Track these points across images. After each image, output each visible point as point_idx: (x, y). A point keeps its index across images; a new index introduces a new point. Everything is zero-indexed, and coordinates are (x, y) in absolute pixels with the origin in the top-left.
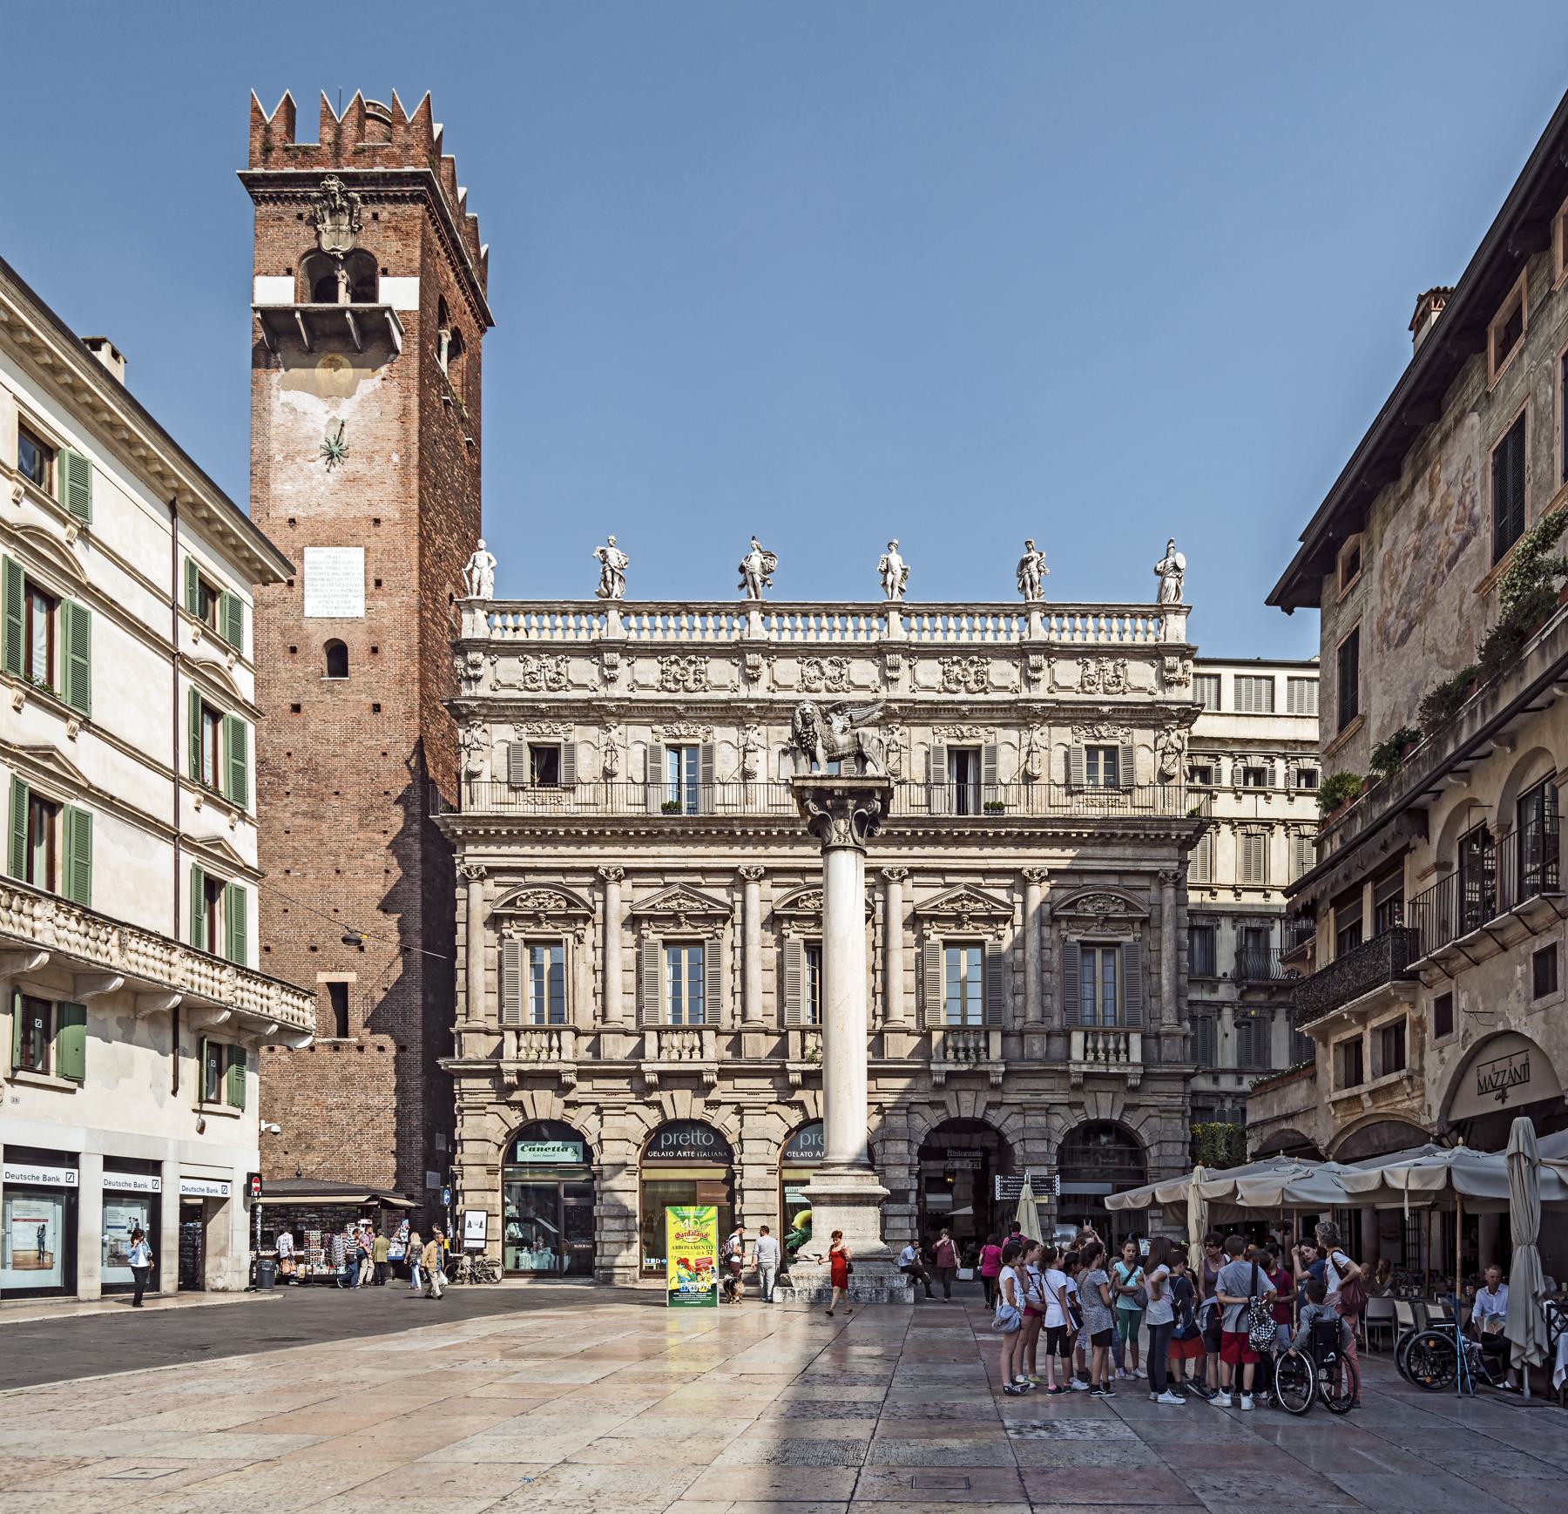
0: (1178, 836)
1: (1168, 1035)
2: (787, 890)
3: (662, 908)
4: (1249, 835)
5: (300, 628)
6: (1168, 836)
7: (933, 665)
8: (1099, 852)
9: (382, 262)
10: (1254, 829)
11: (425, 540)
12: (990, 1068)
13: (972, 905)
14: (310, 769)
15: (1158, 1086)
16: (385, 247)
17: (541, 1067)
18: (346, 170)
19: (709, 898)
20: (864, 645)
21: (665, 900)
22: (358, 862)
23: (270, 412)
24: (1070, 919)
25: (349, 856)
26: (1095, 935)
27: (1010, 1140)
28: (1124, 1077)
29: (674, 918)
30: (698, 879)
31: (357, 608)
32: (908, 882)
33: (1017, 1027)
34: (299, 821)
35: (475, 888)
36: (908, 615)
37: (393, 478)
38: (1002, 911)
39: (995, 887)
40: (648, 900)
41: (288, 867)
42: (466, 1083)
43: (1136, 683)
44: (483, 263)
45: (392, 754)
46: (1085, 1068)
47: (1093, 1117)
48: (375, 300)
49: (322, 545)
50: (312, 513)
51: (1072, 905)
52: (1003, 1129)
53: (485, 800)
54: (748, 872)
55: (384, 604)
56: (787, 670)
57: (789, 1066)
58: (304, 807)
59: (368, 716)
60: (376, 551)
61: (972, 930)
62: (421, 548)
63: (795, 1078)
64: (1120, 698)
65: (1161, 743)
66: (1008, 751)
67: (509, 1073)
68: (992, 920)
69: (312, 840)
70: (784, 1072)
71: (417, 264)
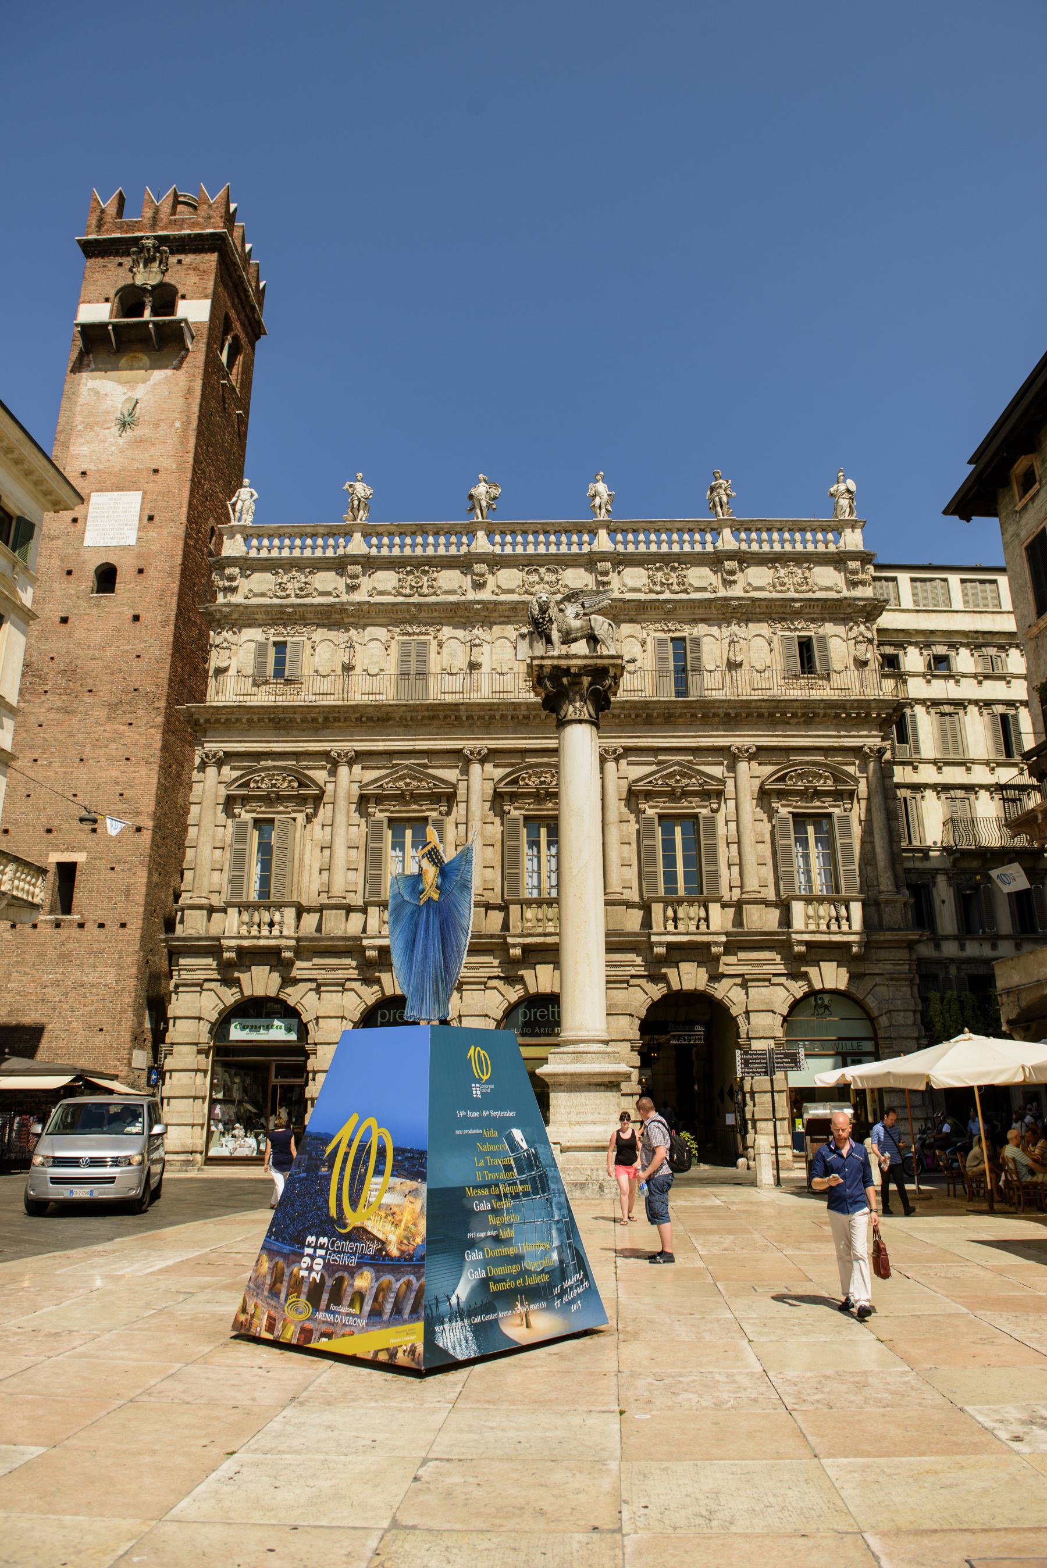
0: (878, 715)
1: (888, 902)
2: (509, 770)
3: (390, 787)
4: (943, 714)
5: (78, 555)
6: (868, 715)
7: (640, 571)
10: (947, 709)
11: (196, 484)
12: (710, 938)
13: (686, 781)
14: (71, 672)
15: (883, 954)
17: (262, 942)
18: (160, 233)
20: (577, 554)
21: (394, 781)
22: (102, 752)
23: (78, 396)
25: (94, 746)
27: (734, 1011)
28: (847, 945)
29: (400, 797)
31: (130, 538)
32: (623, 762)
33: (735, 899)
34: (53, 715)
35: (211, 771)
36: (615, 531)
37: (173, 441)
38: (713, 786)
39: (704, 764)
41: (36, 756)
44: (261, 293)
45: (145, 657)
46: (806, 937)
48: (172, 313)
49: (107, 490)
50: (101, 467)
52: (726, 1001)
53: (226, 692)
54: (472, 753)
55: (154, 534)
56: (509, 577)
57: (510, 940)
58: (59, 704)
59: (128, 623)
60: (152, 493)
61: (686, 804)
62: (192, 491)
63: (516, 952)
64: (810, 595)
65: (852, 634)
66: (713, 644)
67: (229, 949)
69: (62, 732)
70: (505, 947)
71: (210, 290)
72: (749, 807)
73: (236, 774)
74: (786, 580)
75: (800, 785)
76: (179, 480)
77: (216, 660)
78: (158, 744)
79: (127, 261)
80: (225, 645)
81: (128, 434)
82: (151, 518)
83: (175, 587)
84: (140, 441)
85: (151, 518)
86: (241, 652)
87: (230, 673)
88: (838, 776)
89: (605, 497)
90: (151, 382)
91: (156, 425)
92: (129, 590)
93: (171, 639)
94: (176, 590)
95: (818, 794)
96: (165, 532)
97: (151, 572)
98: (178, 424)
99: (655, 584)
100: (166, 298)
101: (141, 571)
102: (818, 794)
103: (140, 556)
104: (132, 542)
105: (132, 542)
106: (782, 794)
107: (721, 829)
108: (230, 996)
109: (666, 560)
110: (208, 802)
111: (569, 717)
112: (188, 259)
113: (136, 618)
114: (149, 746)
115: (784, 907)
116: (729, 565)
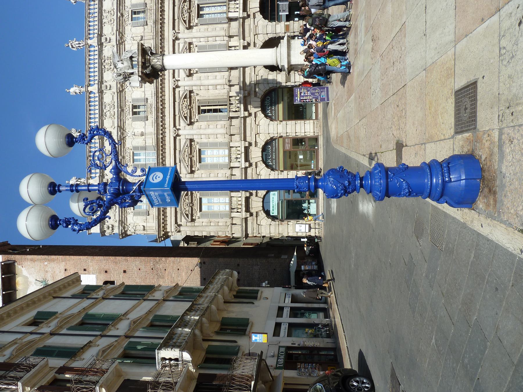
2: (181, 119)
7: (105, 75)
8: (166, 13)
19: (184, 146)
24: (190, 22)
26: (194, 14)
27: (267, 39)
30: (177, 152)
35: (182, 229)
40: (185, 167)
42: (250, 232)
46: (241, 11)
47: (258, 9)
51: (185, 21)
64: (115, 10)
67: (246, 215)
73: (183, 220)
74: (109, 19)
75: (186, 15)
76: (69, 260)
77: (140, 232)
80: (134, 228)
82: (85, 270)
83: (112, 258)
85: (85, 270)
86: (138, 222)
87: (145, 225)
89: (76, 88)
90: (28, 276)
91: (47, 272)
92: (114, 275)
93: (133, 258)
94: (113, 257)
97: (106, 268)
98: (46, 263)
99: (111, 68)
101: (106, 272)
103: (100, 273)
104: (94, 276)
105: (94, 276)
107: (203, 43)
108: (262, 215)
109: (101, 64)
110: (194, 229)
111: (161, 64)
113: (125, 272)
114: (173, 262)
115: (231, 20)
116: (103, 40)
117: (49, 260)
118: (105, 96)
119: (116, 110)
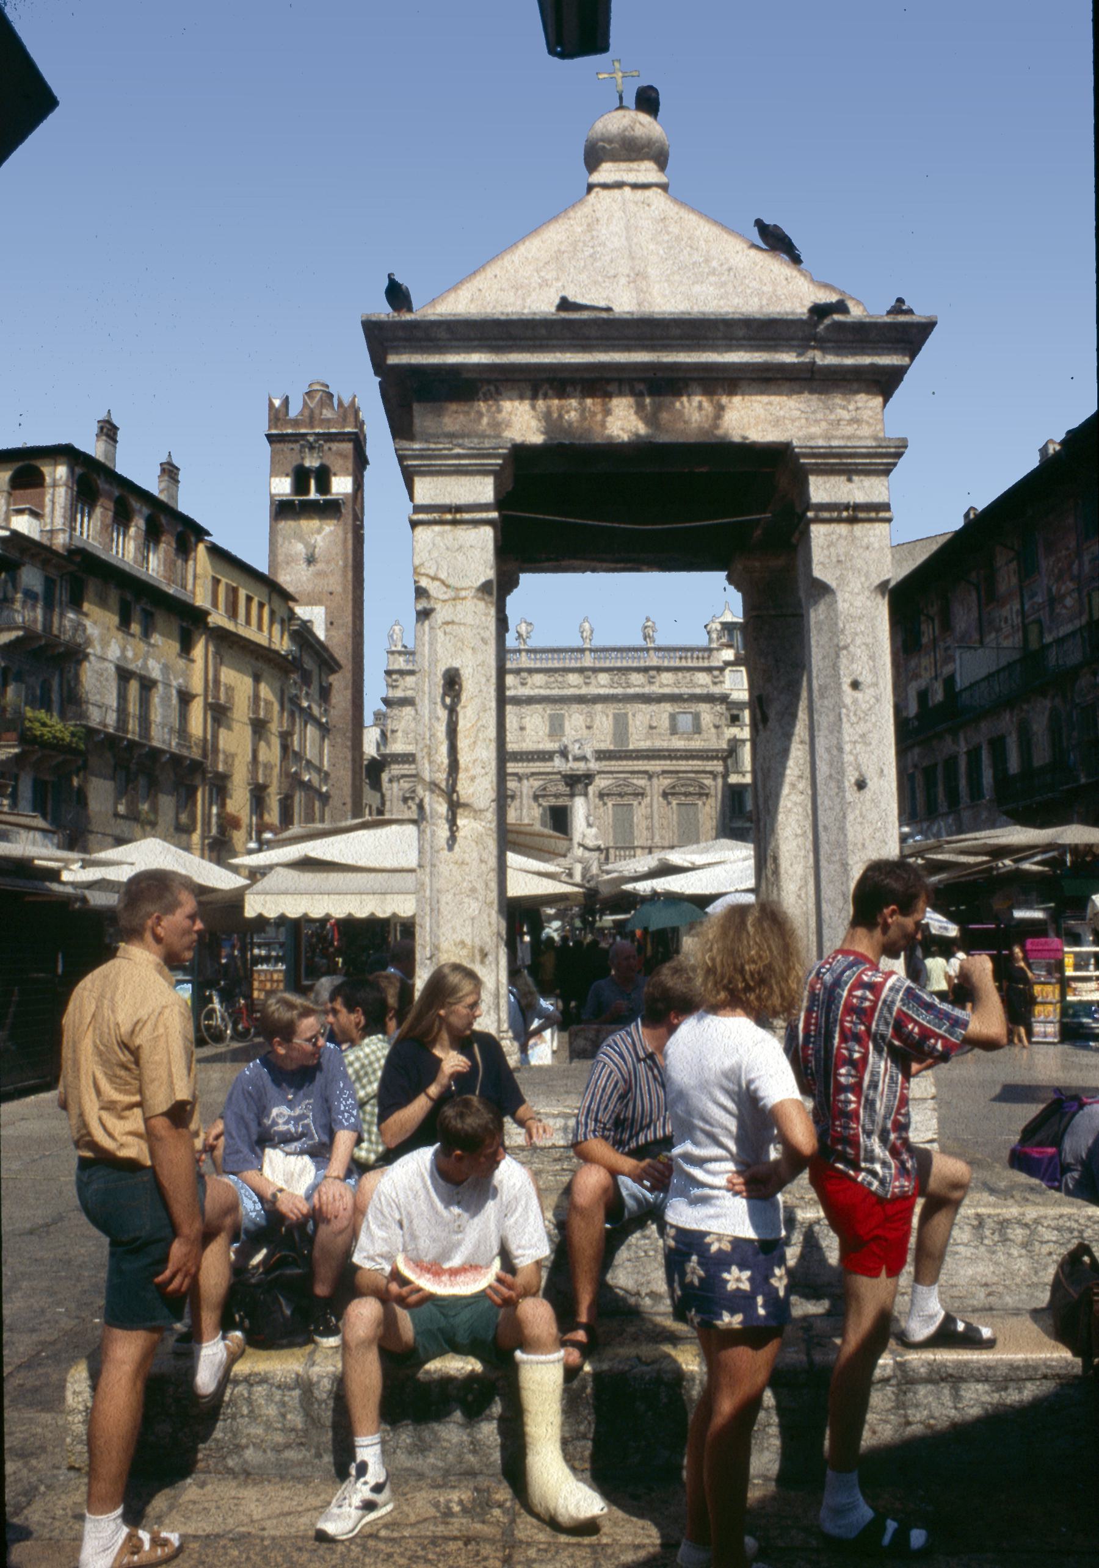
9: (333, 469)
16: (335, 463)
35: (395, 785)
43: (701, 682)
68: (636, 795)
72: (658, 800)
73: (406, 786)
75: (683, 790)
78: (349, 758)
79: (296, 446)
81: (312, 568)
84: (319, 574)
88: (702, 786)
91: (328, 562)
95: (690, 794)
96: (341, 632)
100: (323, 477)
102: (690, 794)
106: (673, 794)
109: (619, 669)
112: (335, 446)
116: (652, 673)
117: (345, 566)
118: (576, 675)
119: (555, 692)
